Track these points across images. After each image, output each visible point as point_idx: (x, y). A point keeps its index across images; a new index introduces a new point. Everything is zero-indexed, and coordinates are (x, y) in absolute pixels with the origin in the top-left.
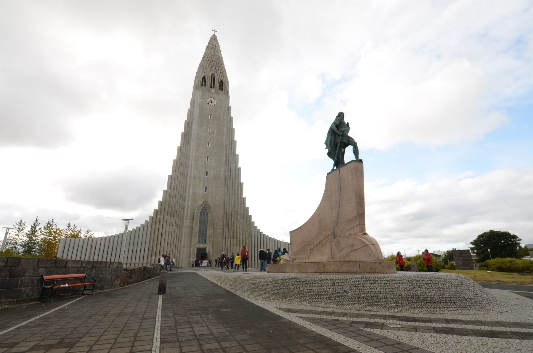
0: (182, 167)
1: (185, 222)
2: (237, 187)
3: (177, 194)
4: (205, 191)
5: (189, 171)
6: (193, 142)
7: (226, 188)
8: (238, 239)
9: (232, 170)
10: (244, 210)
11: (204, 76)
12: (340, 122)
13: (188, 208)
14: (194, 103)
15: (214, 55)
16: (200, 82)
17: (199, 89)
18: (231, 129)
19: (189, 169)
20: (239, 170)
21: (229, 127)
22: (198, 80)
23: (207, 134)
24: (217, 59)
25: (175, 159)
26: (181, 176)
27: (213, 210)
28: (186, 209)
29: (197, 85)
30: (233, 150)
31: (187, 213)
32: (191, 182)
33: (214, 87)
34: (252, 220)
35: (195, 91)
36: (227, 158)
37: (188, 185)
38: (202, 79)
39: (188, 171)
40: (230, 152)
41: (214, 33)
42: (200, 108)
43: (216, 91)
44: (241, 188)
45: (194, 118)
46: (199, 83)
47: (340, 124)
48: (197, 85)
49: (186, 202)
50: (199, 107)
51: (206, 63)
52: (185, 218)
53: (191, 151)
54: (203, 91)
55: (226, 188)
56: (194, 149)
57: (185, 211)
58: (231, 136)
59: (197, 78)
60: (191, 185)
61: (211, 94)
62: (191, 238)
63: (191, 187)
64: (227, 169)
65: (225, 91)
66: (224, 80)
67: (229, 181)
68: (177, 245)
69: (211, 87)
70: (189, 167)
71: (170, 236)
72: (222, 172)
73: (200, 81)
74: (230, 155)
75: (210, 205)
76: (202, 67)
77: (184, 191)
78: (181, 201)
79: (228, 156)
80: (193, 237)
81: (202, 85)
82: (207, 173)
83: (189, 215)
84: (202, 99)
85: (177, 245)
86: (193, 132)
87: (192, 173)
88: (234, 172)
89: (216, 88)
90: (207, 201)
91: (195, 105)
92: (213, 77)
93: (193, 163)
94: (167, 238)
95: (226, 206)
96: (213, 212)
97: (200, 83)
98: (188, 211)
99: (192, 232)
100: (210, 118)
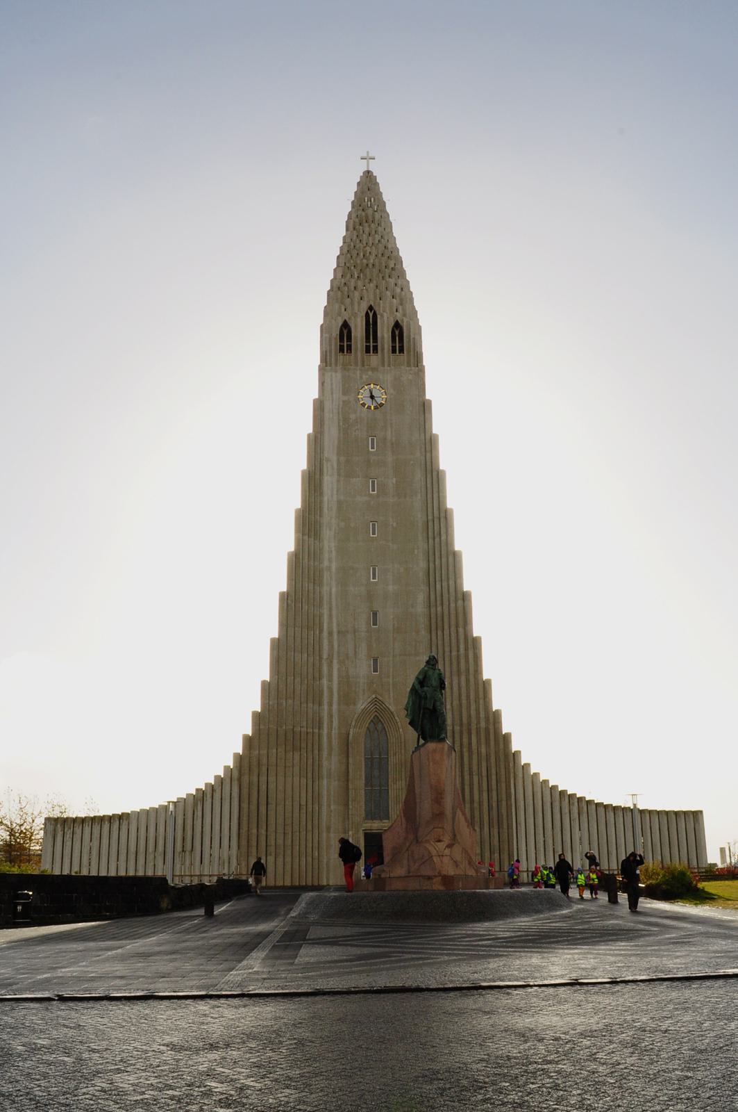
1: (325, 763)
2: (462, 651)
3: (298, 687)
4: (375, 670)
5: (326, 617)
6: (330, 530)
8: (476, 805)
10: (487, 719)
11: (345, 320)
13: (332, 722)
15: (371, 243)
18: (435, 473)
19: (325, 612)
20: (466, 597)
21: (429, 468)
23: (367, 498)
24: (380, 255)
25: (285, 589)
26: (305, 635)
27: (399, 724)
28: (325, 725)
29: (328, 354)
30: (443, 538)
32: (333, 646)
33: (376, 349)
34: (514, 748)
35: (323, 375)
36: (431, 565)
37: (325, 656)
39: (321, 616)
40: (437, 546)
41: (368, 166)
42: (341, 424)
44: (474, 653)
45: (326, 455)
46: (333, 347)
48: (328, 354)
49: (326, 707)
50: (339, 420)
51: (349, 275)
52: (325, 753)
53: (326, 555)
54: (345, 369)
56: (333, 549)
57: (325, 731)
58: (435, 495)
61: (370, 373)
62: (347, 805)
63: (335, 661)
65: (412, 353)
66: (405, 320)
67: (440, 633)
68: (310, 827)
69: (368, 351)
70: (325, 606)
71: (289, 803)
72: (420, 609)
73: (336, 339)
75: (393, 710)
76: (339, 292)
77: (317, 675)
78: (310, 705)
79: (431, 559)
80: (350, 803)
81: (342, 350)
82: (375, 614)
83: (335, 742)
85: (310, 827)
86: (325, 499)
87: (334, 620)
89: (383, 349)
90: (380, 698)
91: (327, 415)
92: (371, 315)
93: (334, 590)
94: (280, 808)
96: (401, 730)
97: (335, 344)
98: (330, 732)
99: (347, 789)
100: (373, 448)
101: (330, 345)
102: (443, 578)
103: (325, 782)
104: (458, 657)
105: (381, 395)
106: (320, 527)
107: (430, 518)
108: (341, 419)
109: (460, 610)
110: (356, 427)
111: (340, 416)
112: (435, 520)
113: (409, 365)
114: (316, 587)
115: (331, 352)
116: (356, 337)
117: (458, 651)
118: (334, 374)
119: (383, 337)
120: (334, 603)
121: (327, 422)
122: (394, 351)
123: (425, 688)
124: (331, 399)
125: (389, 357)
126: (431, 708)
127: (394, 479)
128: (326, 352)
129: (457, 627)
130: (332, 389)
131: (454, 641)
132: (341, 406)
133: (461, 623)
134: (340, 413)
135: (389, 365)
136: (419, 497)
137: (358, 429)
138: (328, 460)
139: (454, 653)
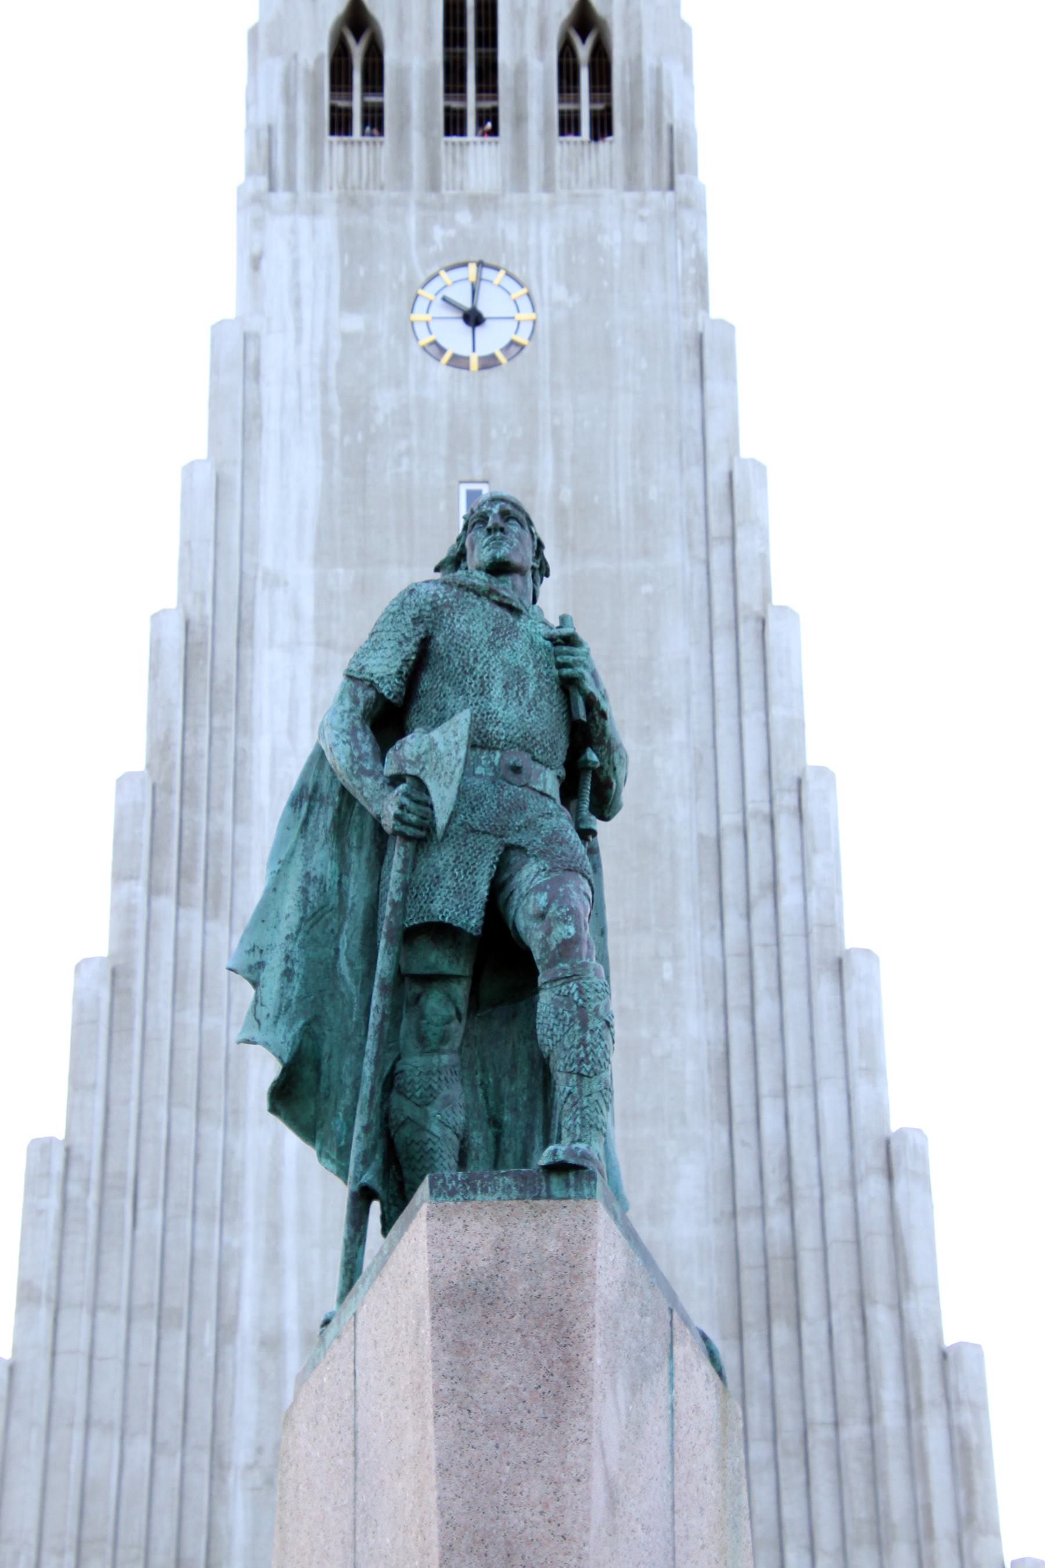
0: (152, 1218)
5: (250, 1269)
9: (805, 1179)
12: (410, 648)
14: (253, 372)
16: (314, 99)
17: (301, 183)
18: (748, 630)
21: (722, 609)
22: (278, 66)
26: (144, 1350)
30: (790, 898)
35: (258, 224)
36: (738, 1025)
38: (324, 48)
40: (761, 936)
42: (336, 429)
43: (519, 162)
44: (950, 1428)
45: (268, 559)
46: (302, 107)
47: (426, 682)
50: (326, 412)
54: (353, 201)
55: (760, 1451)
59: (274, 51)
61: (463, 217)
65: (647, 132)
67: (782, 1334)
69: (454, 124)
73: (315, 75)
74: (764, 980)
81: (340, 124)
88: (838, 1203)
89: (520, 119)
101: (289, 98)
102: (792, 1080)
104: (873, 1446)
105: (512, 311)
106: (234, 864)
107: (730, 818)
108: (337, 410)
109: (875, 1215)
110: (403, 445)
111: (334, 399)
112: (752, 825)
113: (632, 182)
114: (206, 1128)
115: (291, 129)
116: (402, 73)
117: (871, 1419)
118: (304, 223)
119: (521, 71)
121: (272, 423)
122: (568, 125)
123: (412, 745)
124: (291, 325)
125: (548, 153)
126: (472, 921)
128: (270, 129)
129: (862, 1299)
130: (296, 285)
131: (850, 1370)
132: (334, 358)
133: (880, 1283)
134: (333, 384)
135: (548, 186)
136: (679, 734)
137: (409, 452)
138: (275, 581)
139: (854, 1431)
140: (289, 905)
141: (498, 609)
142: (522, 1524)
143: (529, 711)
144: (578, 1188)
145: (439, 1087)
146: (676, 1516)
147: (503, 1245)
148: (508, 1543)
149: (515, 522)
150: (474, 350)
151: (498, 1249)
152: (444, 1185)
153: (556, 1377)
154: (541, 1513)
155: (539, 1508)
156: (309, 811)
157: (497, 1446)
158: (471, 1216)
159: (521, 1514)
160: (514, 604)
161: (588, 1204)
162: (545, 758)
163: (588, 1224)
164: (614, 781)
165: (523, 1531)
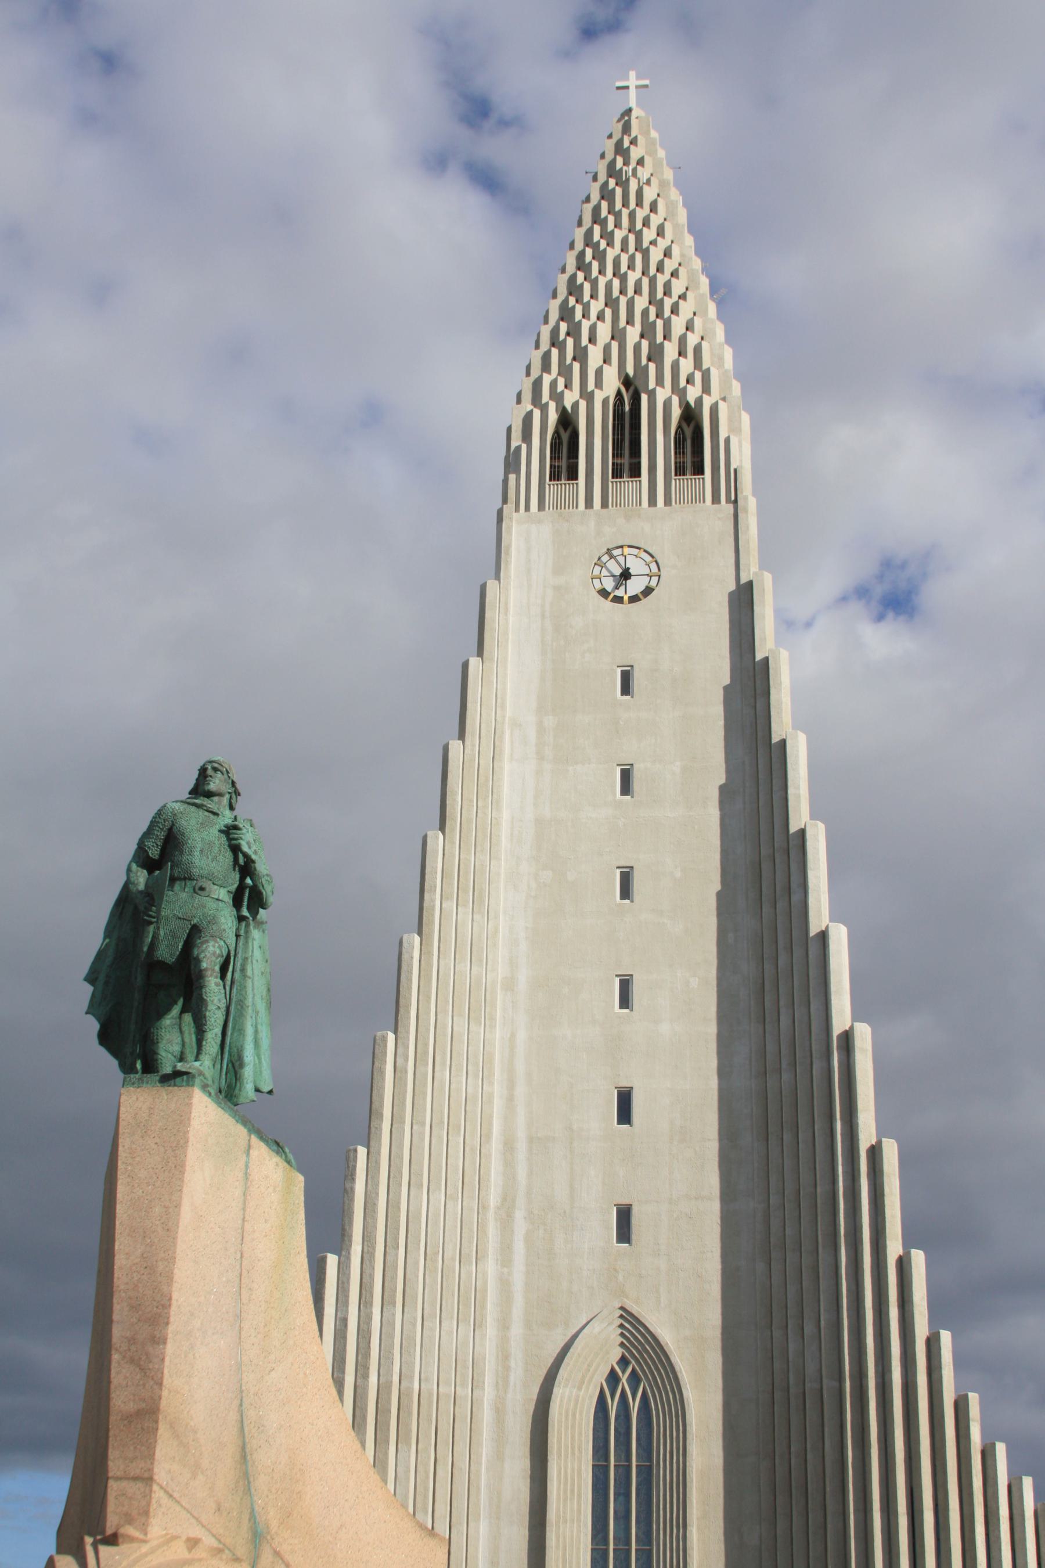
7: (774, 1200)
13: (507, 1369)
19: (497, 1089)
28: (489, 1379)
30: (796, 898)
31: (499, 1411)
36: (768, 967)
37: (493, 1199)
45: (509, 713)
49: (491, 1330)
57: (488, 1394)
60: (521, 1201)
63: (519, 1215)
64: (771, 1048)
66: (707, 402)
84: (558, 569)
86: (506, 815)
95: (777, 1334)
103: (483, 1528)
112: (777, 855)
114: (473, 1028)
120: (520, 1067)
127: (678, 763)
140: (111, 953)
141: (206, 813)
142: (151, 1225)
143: (212, 862)
144: (188, 1081)
145: (165, 1035)
146: (246, 1223)
147: (152, 1107)
148: (145, 1232)
149: (219, 772)
150: (626, 593)
151: (150, 1108)
152: (130, 1079)
153: (170, 1164)
154: (160, 1220)
155: (159, 1218)
156: (123, 908)
157: (143, 1192)
158: (140, 1094)
159: (150, 1221)
160: (214, 811)
161: (190, 1089)
162: (220, 882)
163: (190, 1097)
164: (263, 891)
165: (152, 1227)
